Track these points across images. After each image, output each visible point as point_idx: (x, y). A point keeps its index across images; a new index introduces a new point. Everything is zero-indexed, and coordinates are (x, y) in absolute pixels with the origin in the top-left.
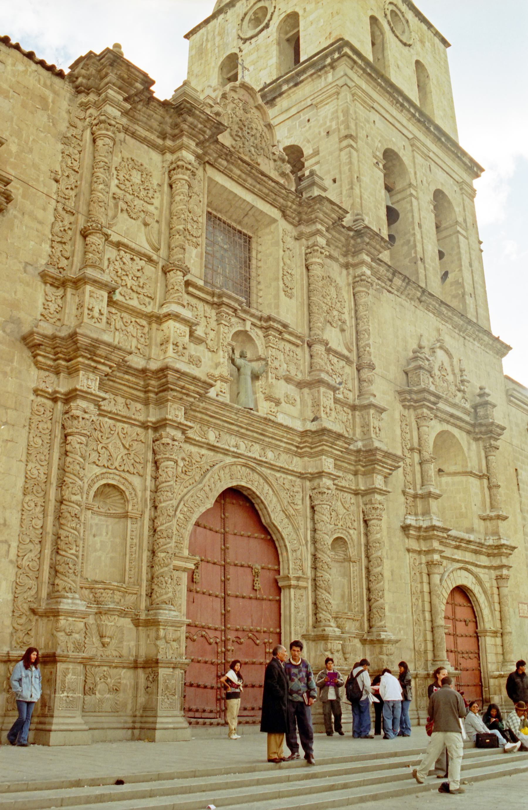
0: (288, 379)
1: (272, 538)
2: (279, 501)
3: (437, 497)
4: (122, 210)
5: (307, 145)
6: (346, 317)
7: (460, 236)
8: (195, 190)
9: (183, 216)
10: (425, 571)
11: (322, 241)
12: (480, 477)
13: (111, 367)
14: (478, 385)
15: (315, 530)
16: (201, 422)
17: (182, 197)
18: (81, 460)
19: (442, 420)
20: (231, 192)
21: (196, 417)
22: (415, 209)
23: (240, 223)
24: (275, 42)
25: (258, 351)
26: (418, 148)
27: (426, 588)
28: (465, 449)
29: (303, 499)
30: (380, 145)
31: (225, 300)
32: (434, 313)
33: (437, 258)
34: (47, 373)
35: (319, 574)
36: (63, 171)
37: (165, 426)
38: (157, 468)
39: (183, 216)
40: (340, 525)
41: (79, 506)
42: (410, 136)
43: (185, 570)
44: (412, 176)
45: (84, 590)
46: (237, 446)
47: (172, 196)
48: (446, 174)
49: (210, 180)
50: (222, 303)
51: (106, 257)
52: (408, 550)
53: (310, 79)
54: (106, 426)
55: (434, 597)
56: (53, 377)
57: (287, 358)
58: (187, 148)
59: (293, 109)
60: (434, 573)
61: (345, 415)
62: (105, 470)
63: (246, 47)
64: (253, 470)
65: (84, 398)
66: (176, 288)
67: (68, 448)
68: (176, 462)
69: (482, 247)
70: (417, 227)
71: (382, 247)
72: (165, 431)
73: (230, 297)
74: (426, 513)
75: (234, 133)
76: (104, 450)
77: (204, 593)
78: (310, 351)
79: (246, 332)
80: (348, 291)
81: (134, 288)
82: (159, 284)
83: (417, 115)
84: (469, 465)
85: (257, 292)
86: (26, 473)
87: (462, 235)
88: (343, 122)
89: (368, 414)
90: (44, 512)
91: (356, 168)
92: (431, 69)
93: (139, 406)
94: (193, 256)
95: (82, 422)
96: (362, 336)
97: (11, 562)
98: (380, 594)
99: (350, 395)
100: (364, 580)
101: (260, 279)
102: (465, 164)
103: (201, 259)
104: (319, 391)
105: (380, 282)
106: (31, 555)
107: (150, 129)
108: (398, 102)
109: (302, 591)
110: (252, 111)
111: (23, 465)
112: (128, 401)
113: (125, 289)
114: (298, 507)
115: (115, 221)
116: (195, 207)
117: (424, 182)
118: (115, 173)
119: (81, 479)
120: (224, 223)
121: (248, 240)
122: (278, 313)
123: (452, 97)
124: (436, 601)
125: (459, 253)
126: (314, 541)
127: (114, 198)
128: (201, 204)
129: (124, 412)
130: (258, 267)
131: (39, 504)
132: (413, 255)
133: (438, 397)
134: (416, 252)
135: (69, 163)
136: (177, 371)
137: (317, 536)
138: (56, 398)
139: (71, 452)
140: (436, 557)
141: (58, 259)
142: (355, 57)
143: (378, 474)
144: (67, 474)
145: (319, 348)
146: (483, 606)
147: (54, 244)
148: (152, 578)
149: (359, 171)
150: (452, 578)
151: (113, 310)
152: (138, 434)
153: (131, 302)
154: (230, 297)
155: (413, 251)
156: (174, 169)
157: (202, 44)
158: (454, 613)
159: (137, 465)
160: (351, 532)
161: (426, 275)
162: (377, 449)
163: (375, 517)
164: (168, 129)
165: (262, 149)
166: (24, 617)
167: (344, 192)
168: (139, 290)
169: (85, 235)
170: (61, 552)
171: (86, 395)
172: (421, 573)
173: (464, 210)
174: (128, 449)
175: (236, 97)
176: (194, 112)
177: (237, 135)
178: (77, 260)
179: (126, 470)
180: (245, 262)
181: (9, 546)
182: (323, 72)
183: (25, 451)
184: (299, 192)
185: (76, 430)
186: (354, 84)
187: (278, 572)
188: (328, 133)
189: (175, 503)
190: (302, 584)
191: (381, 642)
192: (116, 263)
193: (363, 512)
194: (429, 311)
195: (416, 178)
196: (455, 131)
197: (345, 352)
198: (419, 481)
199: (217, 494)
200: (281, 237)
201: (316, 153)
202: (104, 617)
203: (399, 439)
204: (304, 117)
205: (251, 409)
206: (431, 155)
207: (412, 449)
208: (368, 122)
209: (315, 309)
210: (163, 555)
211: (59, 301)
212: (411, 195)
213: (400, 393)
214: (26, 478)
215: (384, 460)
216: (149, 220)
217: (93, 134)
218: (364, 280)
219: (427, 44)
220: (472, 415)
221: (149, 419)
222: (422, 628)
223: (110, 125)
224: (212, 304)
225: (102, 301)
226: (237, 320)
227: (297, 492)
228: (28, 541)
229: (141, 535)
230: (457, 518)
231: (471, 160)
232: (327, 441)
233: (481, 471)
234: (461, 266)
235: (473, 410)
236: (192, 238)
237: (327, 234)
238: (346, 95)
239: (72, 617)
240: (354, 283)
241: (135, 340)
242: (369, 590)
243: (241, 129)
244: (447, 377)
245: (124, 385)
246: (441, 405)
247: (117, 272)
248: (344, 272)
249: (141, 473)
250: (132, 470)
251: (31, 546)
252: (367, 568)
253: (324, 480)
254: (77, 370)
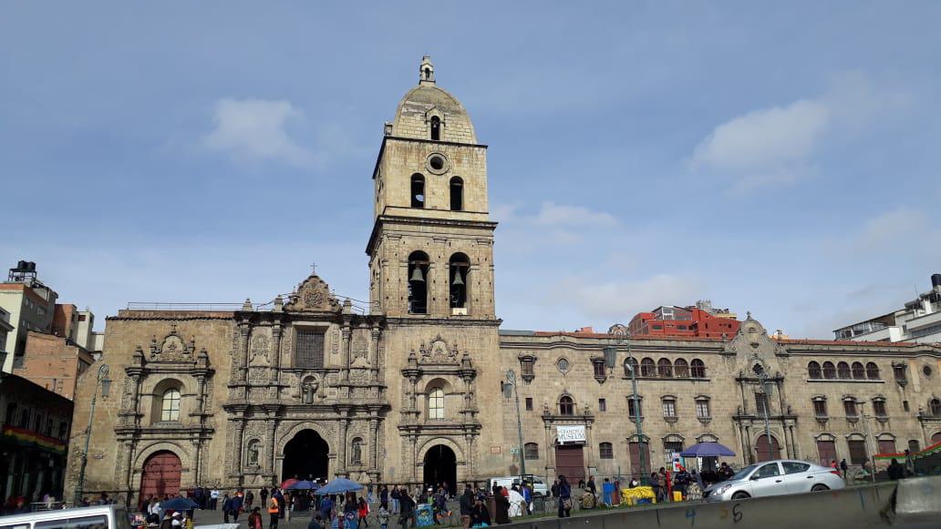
117: (442, 256)
206: (450, 236)
219: (465, 160)
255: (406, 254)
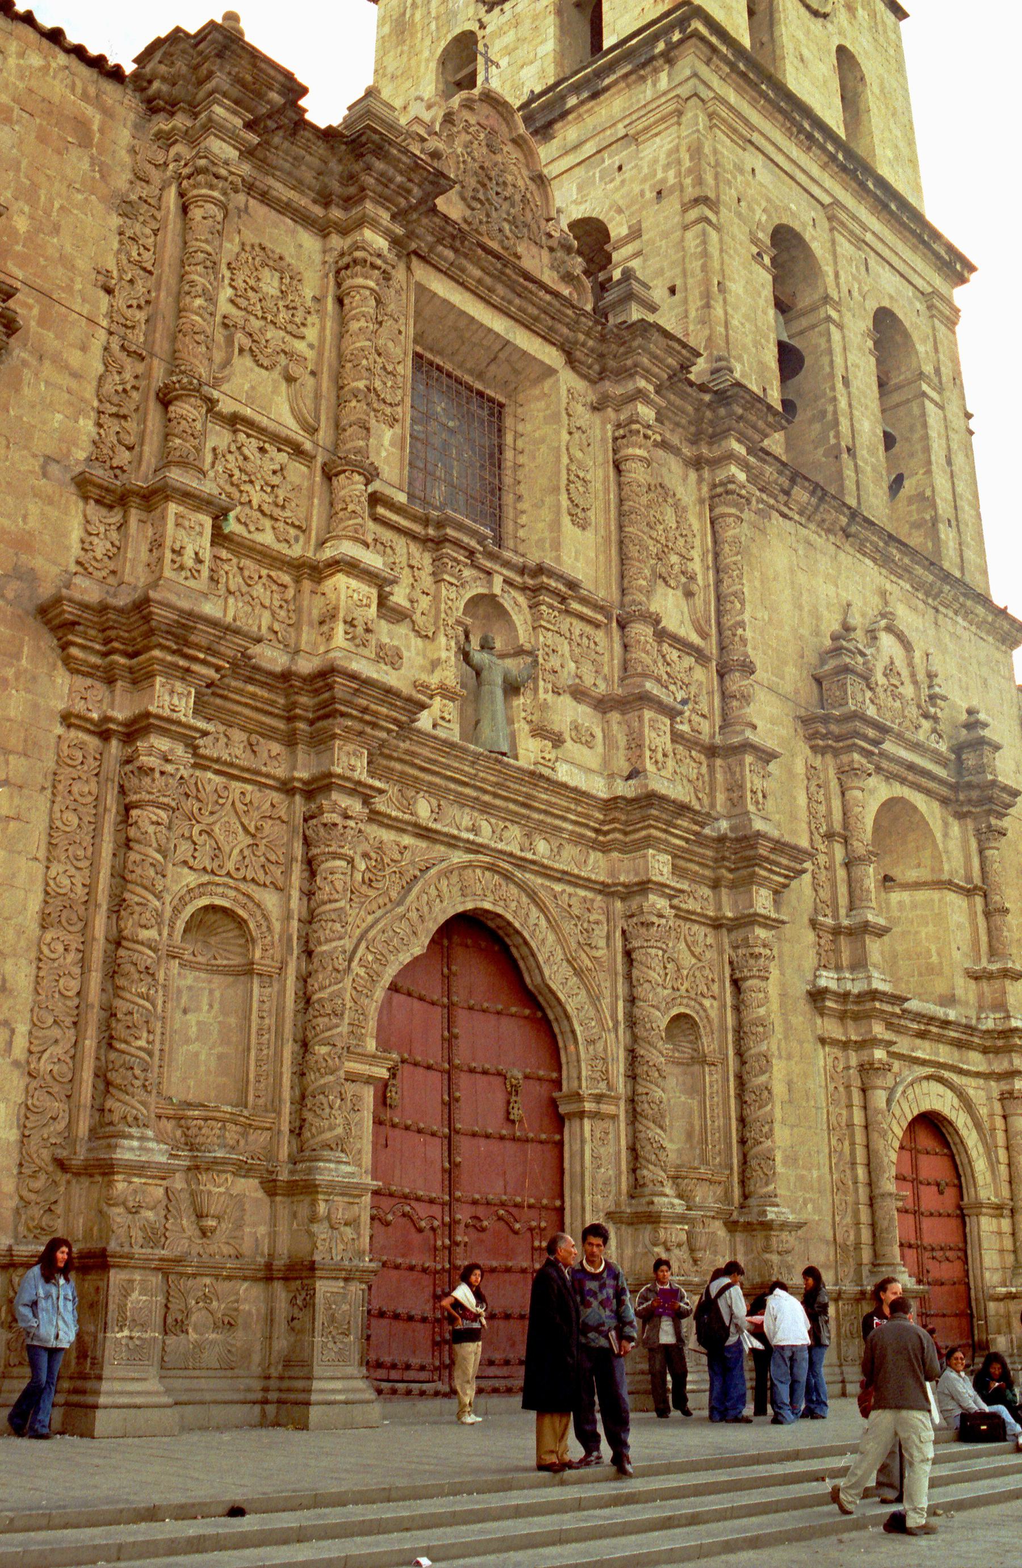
0: (578, 694)
1: (545, 1015)
2: (561, 940)
3: (881, 932)
4: (241, 351)
5: (618, 218)
6: (696, 566)
7: (927, 402)
8: (389, 310)
9: (364, 362)
10: (857, 1082)
11: (646, 412)
12: (969, 893)
13: (218, 669)
14: (965, 706)
15: (632, 1000)
16: (404, 781)
17: (362, 323)
18: (159, 857)
19: (890, 777)
20: (463, 313)
21: (392, 770)
22: (837, 348)
23: (480, 376)
24: (551, 8)
25: (517, 637)
26: (842, 224)
27: (858, 1118)
28: (938, 835)
29: (608, 938)
30: (764, 218)
31: (450, 532)
32: (874, 560)
33: (881, 448)
34: (89, 682)
35: (640, 1090)
36: (121, 271)
37: (328, 788)
38: (313, 874)
39: (364, 362)
40: (683, 988)
41: (155, 950)
42: (827, 200)
43: (369, 1080)
44: (830, 279)
45: (164, 1121)
46: (474, 829)
47: (342, 322)
48: (898, 278)
49: (421, 288)
50: (445, 540)
51: (209, 445)
52: (823, 1041)
53: (622, 85)
54: (208, 789)
55: (875, 1136)
56: (100, 690)
57: (577, 650)
58: (374, 224)
59: (588, 145)
60: (875, 1088)
61: (694, 766)
62: (206, 878)
63: (494, 20)
64: (508, 877)
65: (164, 732)
66: (351, 508)
67: (132, 832)
68: (351, 862)
69: (972, 424)
70: (839, 385)
71: (769, 425)
72: (328, 797)
73: (460, 527)
74: (860, 964)
75: (469, 194)
76: (204, 836)
77: (407, 1128)
78: (623, 636)
79: (494, 596)
80: (701, 515)
81: (265, 507)
82: (316, 501)
83: (840, 157)
84: (946, 867)
85: (516, 517)
86: (47, 884)
87: (932, 400)
88: (690, 171)
89: (741, 764)
90: (84, 963)
91: (716, 265)
92: (870, 66)
93: (276, 748)
94: (386, 442)
95: (160, 781)
96: (729, 606)
97: (16, 1064)
98: (766, 1129)
99: (705, 727)
100: (733, 1101)
101: (522, 489)
102: (937, 256)
103: (403, 449)
104: (640, 718)
105: (764, 496)
106: (58, 1050)
107: (298, 186)
108: (801, 130)
109: (607, 1124)
110: (505, 149)
111: (39, 868)
112: (254, 738)
113: (247, 510)
114: (598, 954)
115: (226, 372)
116: (390, 344)
117: (855, 294)
118: (228, 274)
119: (159, 897)
120: (449, 375)
121: (497, 410)
122: (558, 559)
123: (910, 121)
124: (878, 1144)
125: (926, 437)
126: (632, 1022)
127: (226, 326)
128: (402, 337)
129: (245, 759)
130: (518, 466)
131: (73, 946)
132: (833, 441)
133: (884, 730)
134: (837, 436)
135: (134, 254)
136: (353, 677)
137: (636, 1011)
138: (108, 730)
139: (138, 842)
140: (879, 1054)
141: (112, 449)
142: (714, 40)
143: (761, 885)
144: (130, 886)
145: (641, 631)
146: (974, 1154)
147: (104, 419)
148: (303, 1097)
149: (723, 270)
150: (911, 1097)
151: (224, 554)
152: (273, 805)
153: (259, 538)
154: (460, 527)
155: (832, 434)
156: (347, 267)
157: (404, 14)
158: (915, 1167)
159: (272, 867)
160: (707, 1003)
161: (857, 482)
162: (758, 834)
163: (755, 972)
164: (335, 186)
165: (526, 225)
166: (43, 1177)
167: (693, 314)
168: (277, 512)
169: (165, 400)
170: (118, 1045)
171: (168, 726)
172: (848, 1087)
173: (936, 350)
174: (253, 836)
175: (472, 121)
176: (388, 152)
177: (474, 198)
178: (150, 450)
179: (249, 877)
180: (492, 455)
181: (13, 1032)
182: (648, 69)
183: (44, 838)
184: (601, 314)
185: (148, 797)
186: (712, 95)
187: (558, 1084)
188: (659, 193)
189: (348, 944)
190: (606, 1108)
191: (767, 1226)
192: (229, 457)
193: (731, 963)
194: (864, 554)
195: (838, 285)
196: (918, 189)
197: (695, 638)
198: (843, 901)
199: (433, 927)
200: (564, 405)
201: (635, 233)
202: (204, 1177)
203: (803, 815)
204: (610, 161)
205: (504, 754)
206: (869, 237)
207: (829, 836)
208: (742, 171)
209: (633, 551)
210: (324, 1050)
211: (114, 535)
212: (829, 319)
213: (805, 721)
214: (47, 893)
215: (772, 857)
216: (295, 370)
217: (181, 195)
218: (732, 492)
220: (952, 766)
221: (297, 774)
222: (850, 1199)
223: (217, 176)
224: (424, 541)
225: (201, 534)
226: (474, 572)
227: (597, 923)
228: (51, 1021)
229: (281, 1009)
230: (920, 975)
231: (950, 249)
232: (657, 819)
233: (969, 879)
234: (929, 462)
235: (953, 757)
236: (383, 406)
237: (657, 399)
238: (696, 116)
239: (140, 1176)
240: (712, 498)
241: (267, 614)
242: (742, 1120)
243: (484, 185)
244: (901, 690)
245: (246, 705)
246: (889, 746)
247: (231, 476)
248: (693, 476)
249: (280, 884)
250: (261, 877)
251: (56, 1032)
252: (739, 1078)
253: (652, 897)
254: (151, 676)
255: (765, 221)
